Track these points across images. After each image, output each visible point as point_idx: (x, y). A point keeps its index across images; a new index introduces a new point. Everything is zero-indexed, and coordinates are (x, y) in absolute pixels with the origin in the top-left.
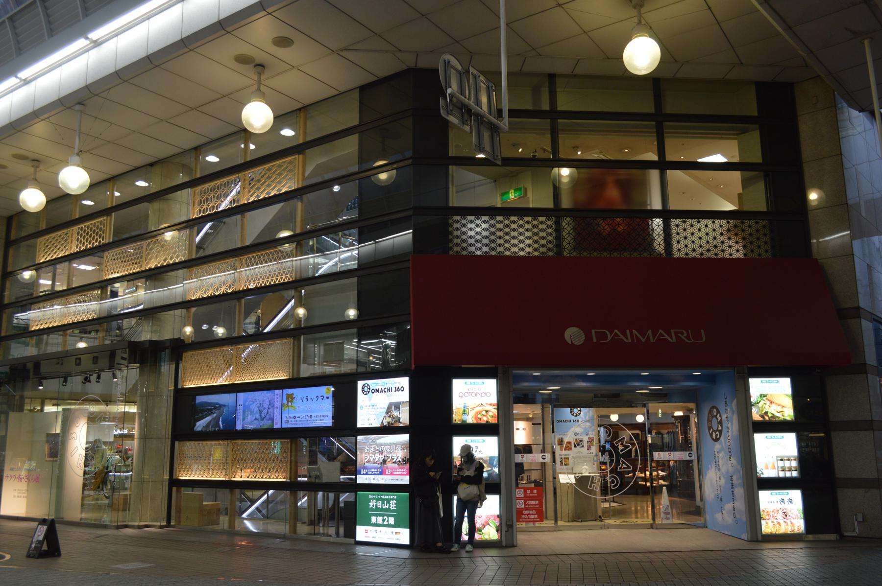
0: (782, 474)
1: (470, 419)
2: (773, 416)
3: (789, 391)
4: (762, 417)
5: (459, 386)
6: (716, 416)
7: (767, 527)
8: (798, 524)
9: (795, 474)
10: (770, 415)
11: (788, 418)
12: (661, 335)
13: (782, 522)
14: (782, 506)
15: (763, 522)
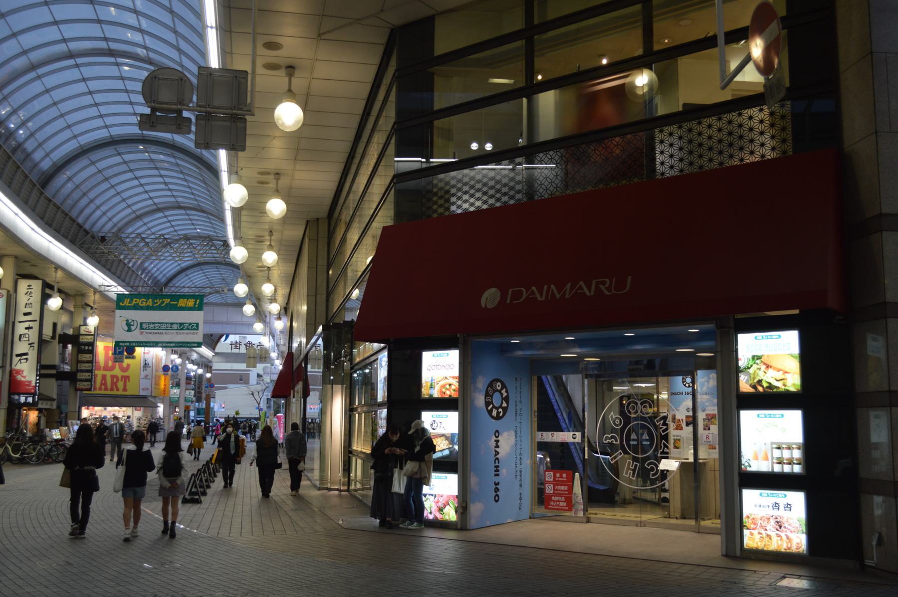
0: (777, 468)
1: (436, 394)
2: (770, 386)
3: (795, 349)
4: (754, 387)
5: (429, 358)
6: (500, 391)
7: (752, 539)
8: (798, 541)
9: (797, 469)
10: (765, 385)
11: (792, 389)
12: (581, 288)
13: (773, 534)
14: (776, 513)
15: (746, 532)
